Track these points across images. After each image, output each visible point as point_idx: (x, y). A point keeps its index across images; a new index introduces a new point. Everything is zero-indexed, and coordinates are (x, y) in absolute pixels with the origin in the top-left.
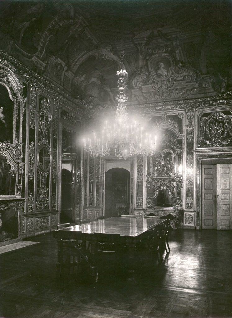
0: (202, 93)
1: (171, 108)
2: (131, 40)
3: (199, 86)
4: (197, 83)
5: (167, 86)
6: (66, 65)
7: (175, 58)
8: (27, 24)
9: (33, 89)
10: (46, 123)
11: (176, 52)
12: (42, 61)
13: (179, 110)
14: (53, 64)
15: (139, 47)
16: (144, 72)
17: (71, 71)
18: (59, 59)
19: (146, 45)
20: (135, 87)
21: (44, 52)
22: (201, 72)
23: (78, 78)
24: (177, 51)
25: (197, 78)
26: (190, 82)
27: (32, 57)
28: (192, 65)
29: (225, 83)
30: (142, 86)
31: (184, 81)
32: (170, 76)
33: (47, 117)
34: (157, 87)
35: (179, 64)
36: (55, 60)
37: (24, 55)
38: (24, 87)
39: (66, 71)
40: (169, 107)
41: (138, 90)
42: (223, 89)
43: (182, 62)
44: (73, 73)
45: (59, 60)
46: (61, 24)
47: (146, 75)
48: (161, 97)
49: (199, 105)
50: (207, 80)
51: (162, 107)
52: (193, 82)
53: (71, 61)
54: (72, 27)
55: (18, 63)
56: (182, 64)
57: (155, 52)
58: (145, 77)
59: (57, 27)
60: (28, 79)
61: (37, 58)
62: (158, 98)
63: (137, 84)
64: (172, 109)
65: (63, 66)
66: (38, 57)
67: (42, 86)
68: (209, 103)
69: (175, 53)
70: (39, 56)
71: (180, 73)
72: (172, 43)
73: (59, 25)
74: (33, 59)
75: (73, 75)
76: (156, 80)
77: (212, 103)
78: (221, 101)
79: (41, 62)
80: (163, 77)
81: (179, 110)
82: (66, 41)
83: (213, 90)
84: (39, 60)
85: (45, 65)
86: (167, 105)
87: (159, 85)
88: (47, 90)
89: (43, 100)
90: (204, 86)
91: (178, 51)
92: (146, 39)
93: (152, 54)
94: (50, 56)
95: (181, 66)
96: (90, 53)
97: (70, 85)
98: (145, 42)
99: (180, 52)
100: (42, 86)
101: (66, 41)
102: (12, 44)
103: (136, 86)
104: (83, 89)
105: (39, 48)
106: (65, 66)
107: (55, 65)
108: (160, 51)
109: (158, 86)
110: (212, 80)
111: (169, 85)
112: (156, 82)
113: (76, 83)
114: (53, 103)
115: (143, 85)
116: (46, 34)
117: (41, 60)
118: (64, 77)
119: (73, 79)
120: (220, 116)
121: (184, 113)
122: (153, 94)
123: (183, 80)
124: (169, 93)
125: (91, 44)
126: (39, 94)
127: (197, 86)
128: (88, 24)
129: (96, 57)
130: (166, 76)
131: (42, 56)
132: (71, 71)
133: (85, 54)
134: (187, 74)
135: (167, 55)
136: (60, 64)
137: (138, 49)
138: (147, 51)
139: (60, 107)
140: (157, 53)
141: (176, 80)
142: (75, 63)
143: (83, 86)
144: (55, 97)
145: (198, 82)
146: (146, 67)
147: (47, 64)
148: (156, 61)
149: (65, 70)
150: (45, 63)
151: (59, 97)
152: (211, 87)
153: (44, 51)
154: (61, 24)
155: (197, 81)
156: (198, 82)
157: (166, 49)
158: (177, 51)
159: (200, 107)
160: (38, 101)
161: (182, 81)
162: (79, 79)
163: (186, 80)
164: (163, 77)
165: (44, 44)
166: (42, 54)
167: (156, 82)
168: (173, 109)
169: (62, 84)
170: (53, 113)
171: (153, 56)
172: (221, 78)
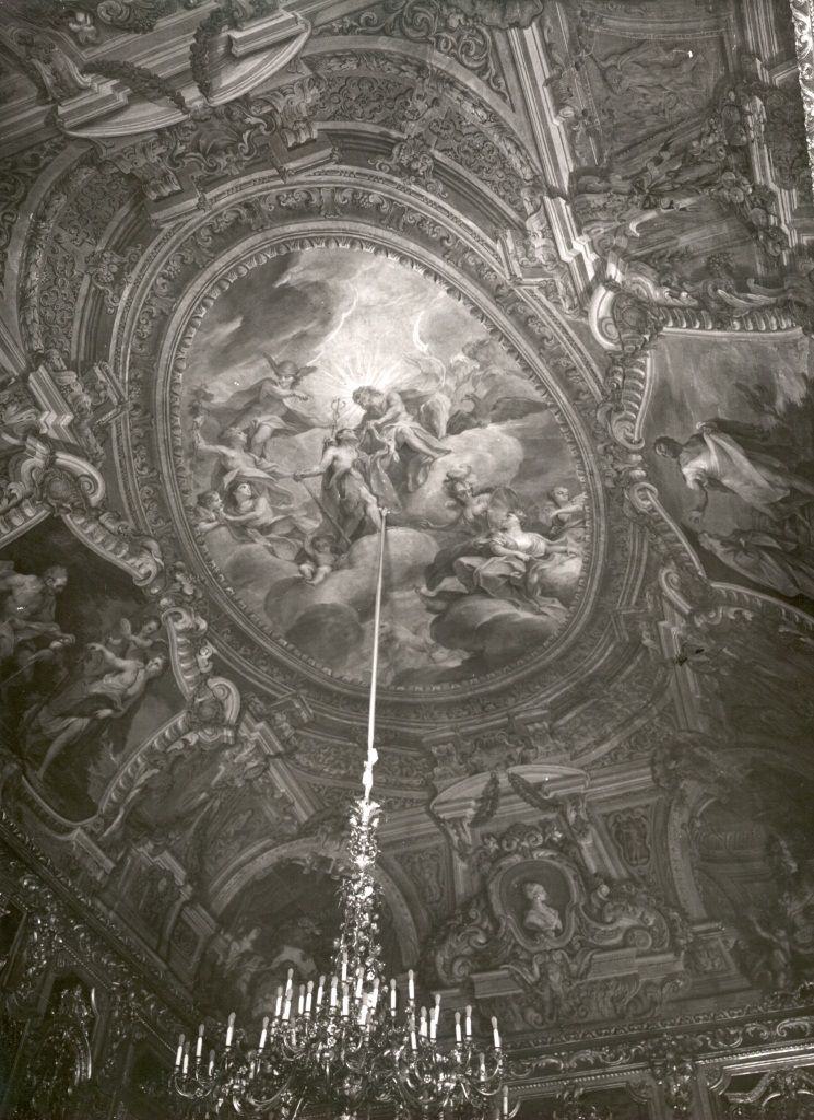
0: (708, 996)
1: (597, 1060)
2: (423, 809)
3: (686, 966)
4: (677, 954)
5: (569, 971)
6: (188, 881)
7: (581, 868)
8: (79, 723)
9: (40, 933)
10: (57, 1086)
11: (583, 843)
12: (104, 850)
13: (626, 1067)
14: (143, 869)
15: (452, 832)
16: (477, 922)
17: (207, 907)
18: (166, 855)
19: (476, 822)
20: (444, 980)
21: (118, 820)
22: (684, 914)
23: (228, 937)
24: (586, 843)
25: (673, 937)
26: (652, 953)
27: (69, 830)
28: (645, 889)
29: (783, 950)
30: (475, 976)
31: (628, 951)
32: (575, 934)
33: (70, 1063)
34: (531, 979)
35: (597, 888)
36: (153, 856)
37: (44, 818)
38: (7, 916)
39: (186, 904)
40: (588, 1055)
41: (457, 991)
42: (783, 976)
43: (609, 881)
44: (213, 915)
45: (166, 860)
46: (192, 738)
47: (486, 931)
48: (551, 1017)
49: (705, 1042)
50: (713, 945)
51: (559, 1057)
52: (661, 953)
53: (209, 868)
54: (227, 753)
55: (12, 828)
56: (610, 886)
57: (508, 846)
58: (482, 940)
59: (179, 745)
60: (32, 895)
61: (85, 837)
62: (540, 1020)
63: (452, 966)
64: (598, 1064)
65: (180, 881)
66: (91, 834)
67: (82, 935)
68: (745, 1034)
69: (580, 848)
70: (97, 831)
71: (609, 919)
72: (564, 814)
73: (186, 742)
74: (73, 836)
75: (212, 921)
76: (523, 949)
77: (756, 1032)
78: (787, 1023)
79: (99, 852)
80: (547, 936)
81: (626, 1067)
82: (203, 795)
83: (745, 983)
84: (93, 846)
85: (111, 865)
86: (577, 1048)
87: (536, 970)
88: (97, 958)
89: (72, 989)
90: (709, 968)
91: (589, 842)
92: (473, 803)
93: (501, 855)
94: (136, 840)
95: (609, 896)
96: (283, 851)
97: (195, 959)
98: (471, 812)
99: (594, 845)
100: (82, 935)
101: (203, 795)
102: (12, 772)
103: (450, 973)
104: (244, 988)
105: (104, 806)
106: (185, 886)
107: (151, 873)
108: (525, 844)
109: (531, 972)
110: (732, 942)
111: (574, 968)
112: (523, 956)
113: (221, 958)
114: (112, 1012)
115: (477, 971)
116: (136, 764)
117: (100, 847)
118: (176, 924)
119: (211, 939)
120: (800, 1087)
121: (650, 1081)
122: (515, 1007)
123: (624, 945)
124: (577, 1000)
125: (288, 818)
126: (62, 964)
127: (680, 967)
128: (280, 749)
129: (303, 868)
130: (557, 931)
131: (105, 834)
132: (204, 907)
133: (265, 849)
134: (636, 923)
135: (552, 857)
136: (170, 876)
137: (448, 837)
138: (480, 844)
139: (138, 1036)
140: (516, 851)
141: (598, 947)
142: (224, 882)
143: (247, 977)
144: (123, 988)
145: (683, 953)
146: (482, 901)
147: (120, 864)
148: (517, 879)
149: (183, 899)
150: (114, 861)
151: (140, 998)
152: (734, 971)
153: (120, 816)
154: (192, 738)
155: (675, 949)
156: (683, 953)
157: (544, 835)
158: (586, 843)
159: (710, 1050)
160: (49, 987)
161: (620, 952)
162: (235, 945)
163: (634, 946)
164: (547, 936)
165: (124, 793)
166: (108, 824)
167: (523, 956)
168: (608, 1066)
169: (163, 950)
170: (101, 1053)
171: (504, 863)
172: (764, 934)
